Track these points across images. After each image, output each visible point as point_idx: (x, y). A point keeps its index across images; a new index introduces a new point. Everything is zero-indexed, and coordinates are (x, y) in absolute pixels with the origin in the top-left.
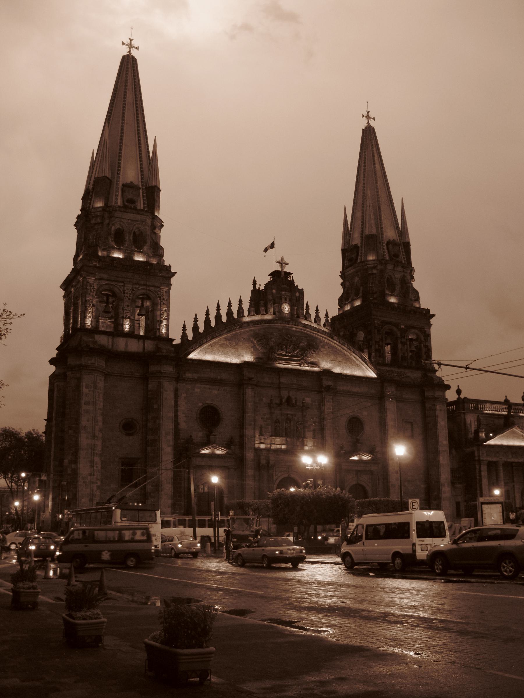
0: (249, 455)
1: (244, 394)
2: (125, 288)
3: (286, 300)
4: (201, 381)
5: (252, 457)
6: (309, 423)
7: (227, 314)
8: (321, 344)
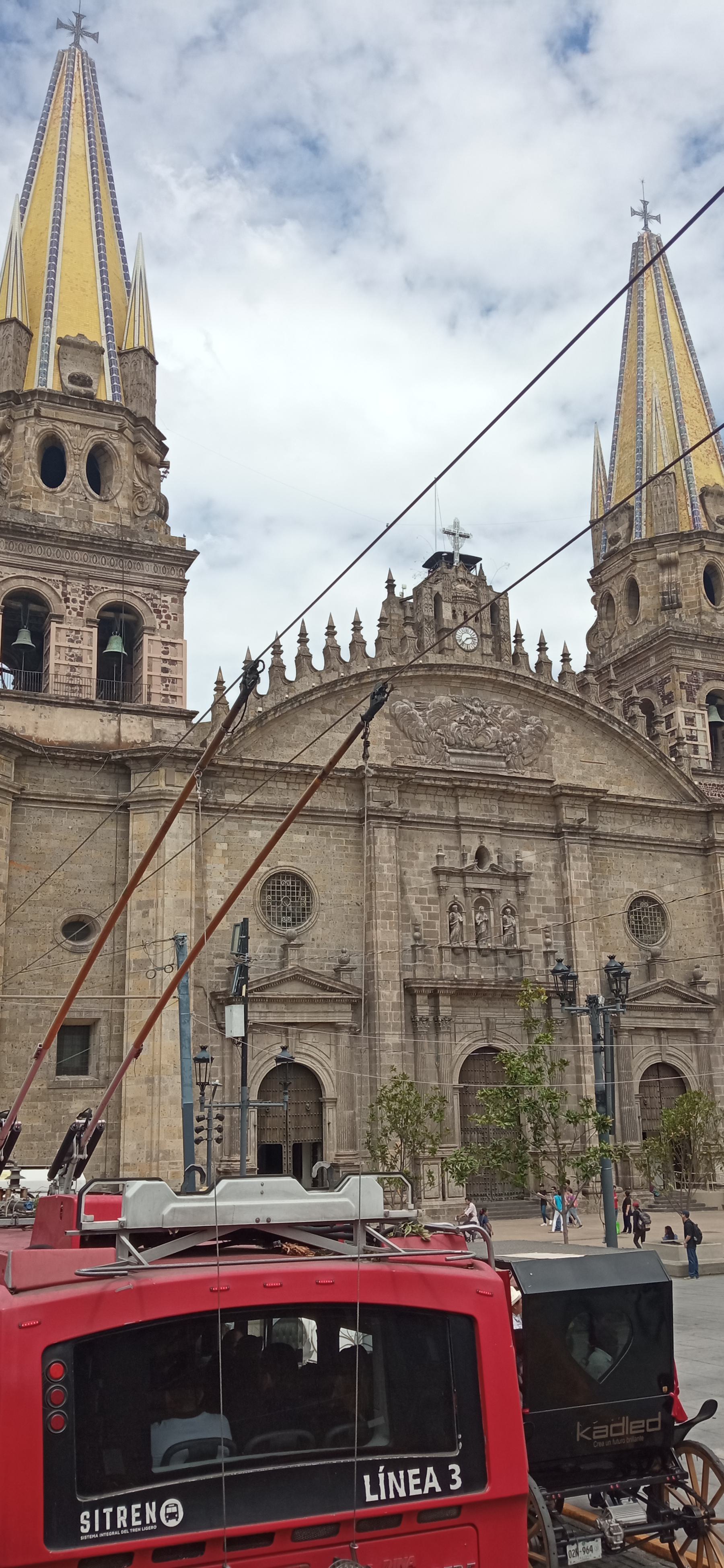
0: (387, 993)
1: (372, 842)
2: (69, 588)
5: (395, 1000)
6: (533, 912)
7: (326, 652)
8: (556, 723)
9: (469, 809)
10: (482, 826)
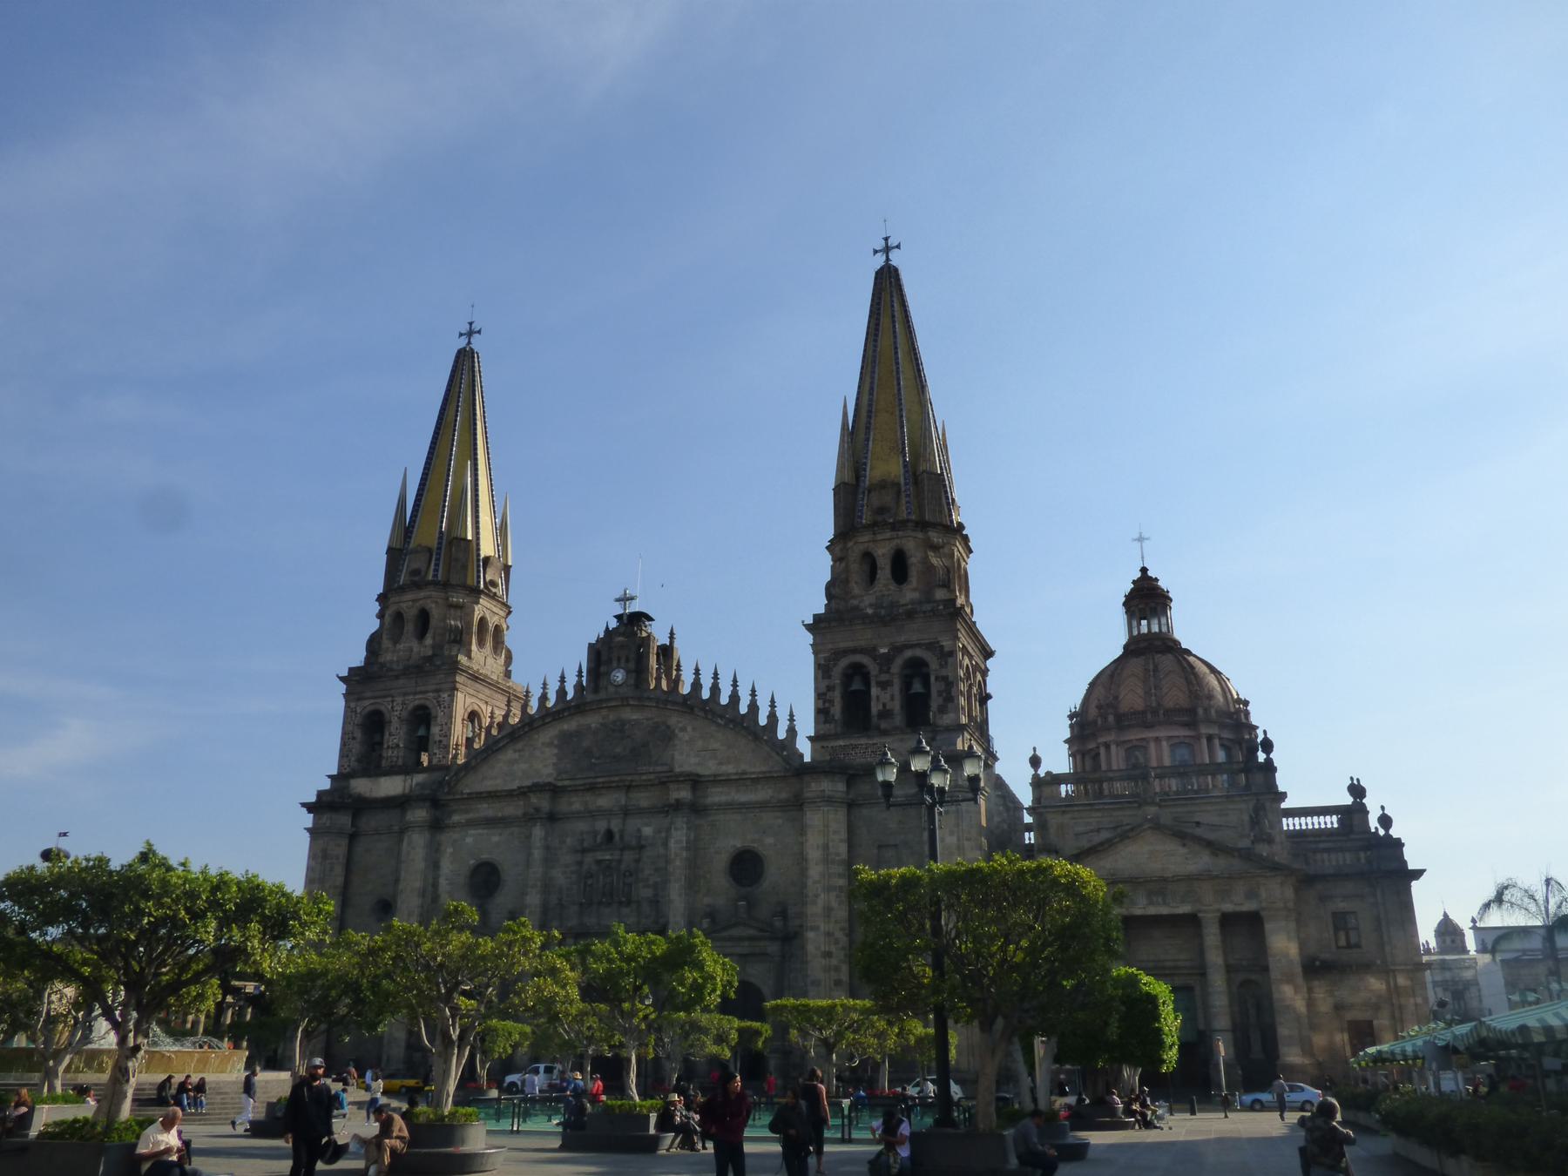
1: (529, 836)
3: (619, 659)
4: (471, 824)
10: (607, 813)
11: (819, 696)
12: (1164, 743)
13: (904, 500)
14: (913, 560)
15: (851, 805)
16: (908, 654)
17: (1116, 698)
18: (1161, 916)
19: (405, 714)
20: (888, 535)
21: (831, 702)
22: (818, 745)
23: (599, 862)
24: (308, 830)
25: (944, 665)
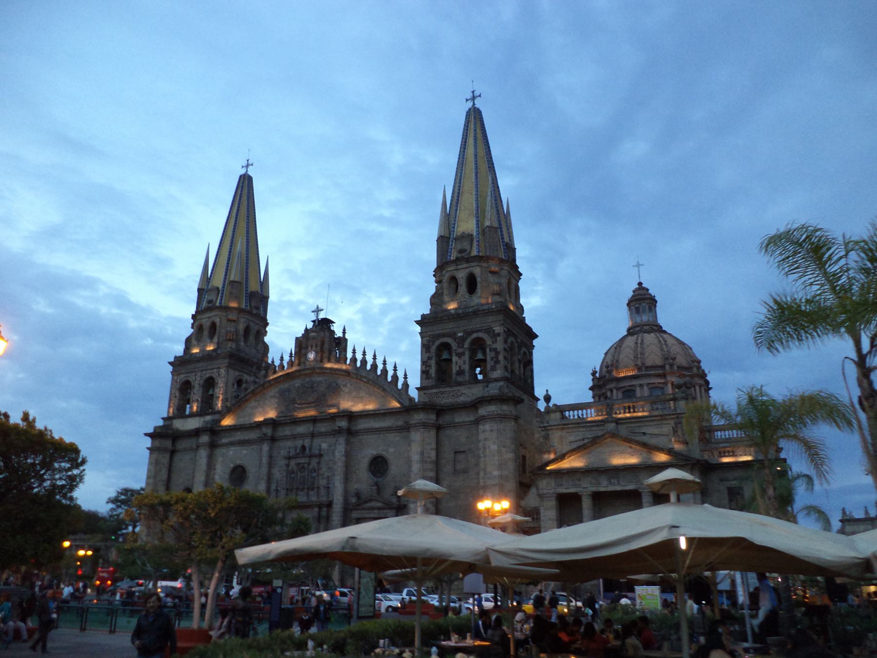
4: (232, 444)
9: (301, 429)
10: (302, 436)
11: (423, 363)
12: (645, 387)
13: (475, 244)
14: (478, 280)
15: (439, 428)
16: (475, 335)
17: (617, 361)
18: (626, 491)
19: (202, 382)
20: (465, 266)
21: (430, 366)
22: (422, 393)
23: (298, 464)
24: (148, 448)
25: (495, 342)
